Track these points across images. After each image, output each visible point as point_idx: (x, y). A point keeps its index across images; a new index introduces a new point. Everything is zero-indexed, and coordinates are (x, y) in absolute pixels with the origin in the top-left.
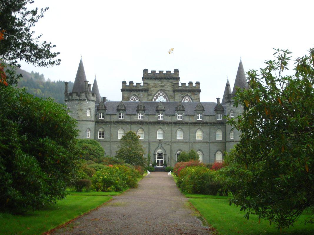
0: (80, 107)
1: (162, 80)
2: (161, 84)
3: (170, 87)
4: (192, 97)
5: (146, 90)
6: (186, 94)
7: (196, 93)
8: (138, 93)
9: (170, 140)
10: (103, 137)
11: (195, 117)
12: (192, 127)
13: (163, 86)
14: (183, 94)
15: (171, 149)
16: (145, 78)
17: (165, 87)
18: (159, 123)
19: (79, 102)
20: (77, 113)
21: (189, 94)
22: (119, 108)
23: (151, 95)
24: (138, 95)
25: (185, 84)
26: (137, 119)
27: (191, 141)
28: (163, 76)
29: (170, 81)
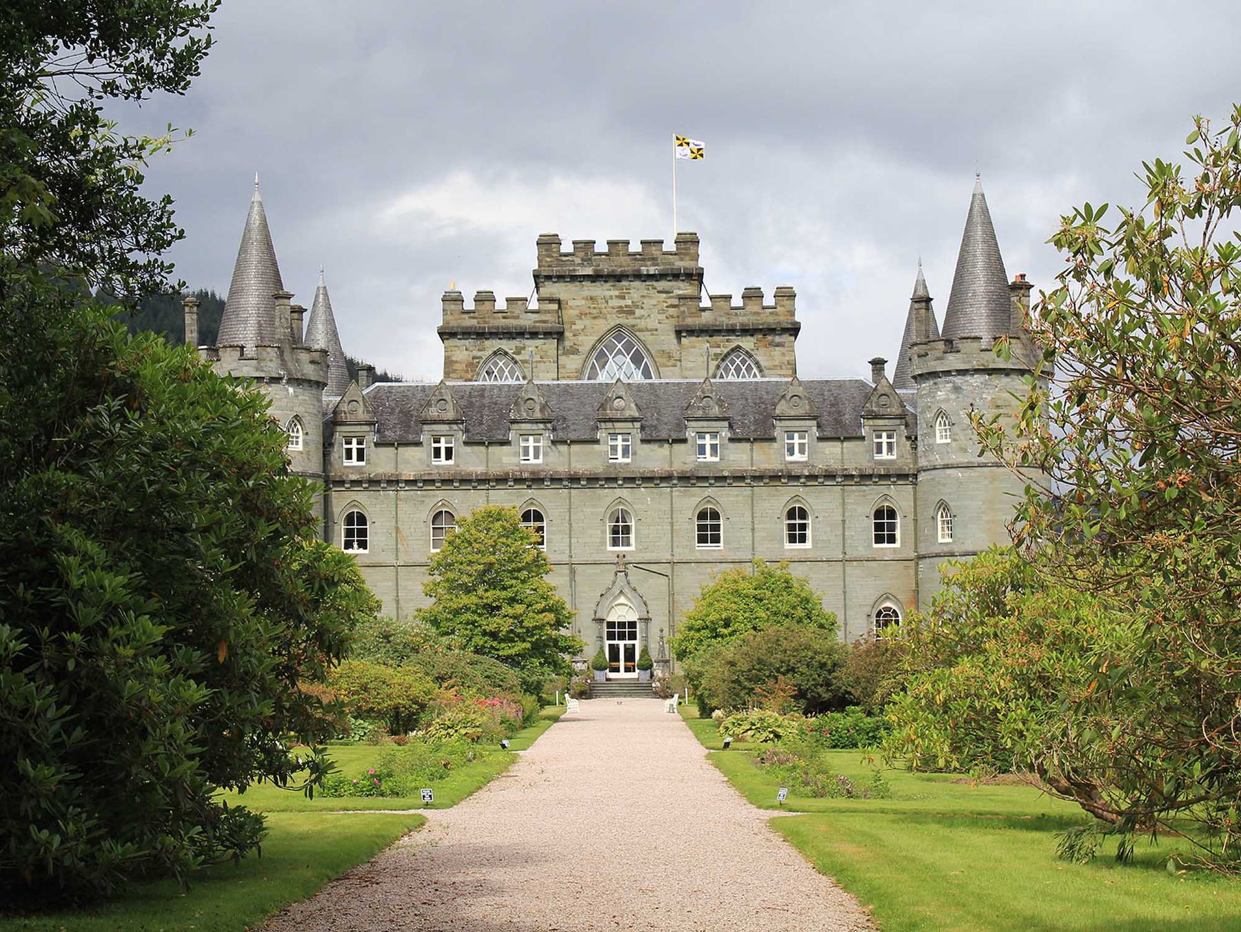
1: (624, 283)
2: (622, 303)
3: (662, 312)
4: (758, 358)
6: (734, 345)
7: (777, 339)
8: (517, 343)
9: (668, 557)
10: (363, 545)
11: (775, 445)
12: (762, 491)
13: (629, 312)
14: (719, 346)
15: (671, 594)
16: (548, 278)
17: (638, 312)
21: (747, 343)
22: (433, 412)
23: (575, 351)
24: (518, 353)
25: (728, 298)
26: (514, 460)
28: (621, 264)
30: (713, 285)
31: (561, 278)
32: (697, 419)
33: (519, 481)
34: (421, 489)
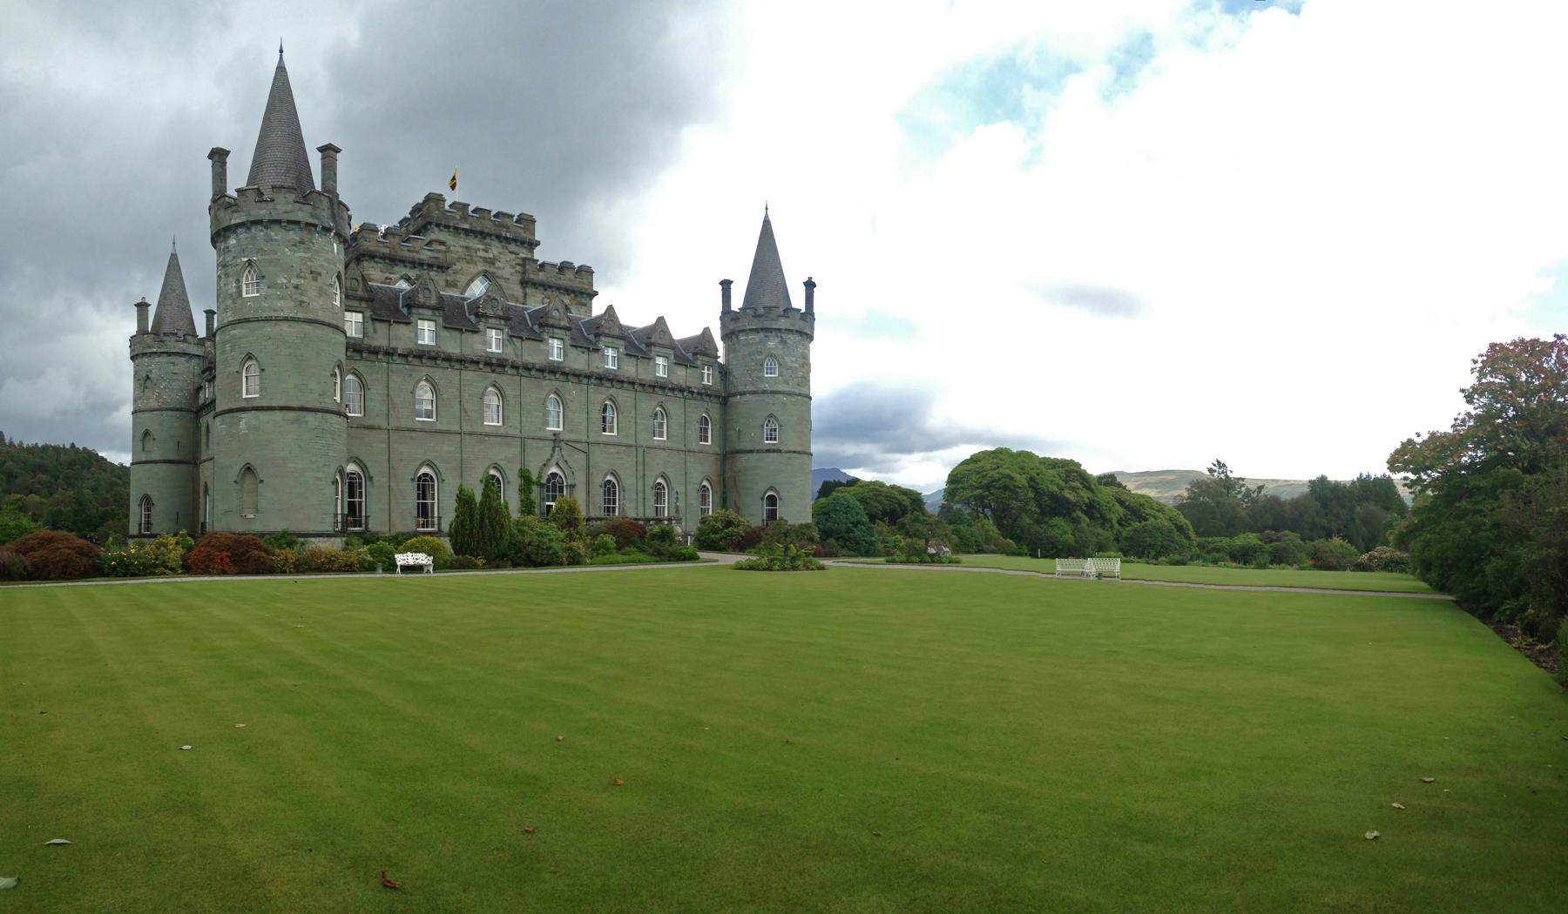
0: (310, 259)
5: (443, 268)
13: (491, 262)
18: (553, 370)
19: (305, 235)
20: (296, 287)
21: (567, 299)
27: (641, 443)
28: (488, 226)
29: (513, 247)
30: (540, 255)
31: (447, 227)
32: (607, 335)
33: (488, 364)
34: (408, 363)
